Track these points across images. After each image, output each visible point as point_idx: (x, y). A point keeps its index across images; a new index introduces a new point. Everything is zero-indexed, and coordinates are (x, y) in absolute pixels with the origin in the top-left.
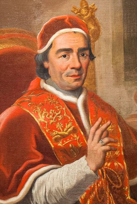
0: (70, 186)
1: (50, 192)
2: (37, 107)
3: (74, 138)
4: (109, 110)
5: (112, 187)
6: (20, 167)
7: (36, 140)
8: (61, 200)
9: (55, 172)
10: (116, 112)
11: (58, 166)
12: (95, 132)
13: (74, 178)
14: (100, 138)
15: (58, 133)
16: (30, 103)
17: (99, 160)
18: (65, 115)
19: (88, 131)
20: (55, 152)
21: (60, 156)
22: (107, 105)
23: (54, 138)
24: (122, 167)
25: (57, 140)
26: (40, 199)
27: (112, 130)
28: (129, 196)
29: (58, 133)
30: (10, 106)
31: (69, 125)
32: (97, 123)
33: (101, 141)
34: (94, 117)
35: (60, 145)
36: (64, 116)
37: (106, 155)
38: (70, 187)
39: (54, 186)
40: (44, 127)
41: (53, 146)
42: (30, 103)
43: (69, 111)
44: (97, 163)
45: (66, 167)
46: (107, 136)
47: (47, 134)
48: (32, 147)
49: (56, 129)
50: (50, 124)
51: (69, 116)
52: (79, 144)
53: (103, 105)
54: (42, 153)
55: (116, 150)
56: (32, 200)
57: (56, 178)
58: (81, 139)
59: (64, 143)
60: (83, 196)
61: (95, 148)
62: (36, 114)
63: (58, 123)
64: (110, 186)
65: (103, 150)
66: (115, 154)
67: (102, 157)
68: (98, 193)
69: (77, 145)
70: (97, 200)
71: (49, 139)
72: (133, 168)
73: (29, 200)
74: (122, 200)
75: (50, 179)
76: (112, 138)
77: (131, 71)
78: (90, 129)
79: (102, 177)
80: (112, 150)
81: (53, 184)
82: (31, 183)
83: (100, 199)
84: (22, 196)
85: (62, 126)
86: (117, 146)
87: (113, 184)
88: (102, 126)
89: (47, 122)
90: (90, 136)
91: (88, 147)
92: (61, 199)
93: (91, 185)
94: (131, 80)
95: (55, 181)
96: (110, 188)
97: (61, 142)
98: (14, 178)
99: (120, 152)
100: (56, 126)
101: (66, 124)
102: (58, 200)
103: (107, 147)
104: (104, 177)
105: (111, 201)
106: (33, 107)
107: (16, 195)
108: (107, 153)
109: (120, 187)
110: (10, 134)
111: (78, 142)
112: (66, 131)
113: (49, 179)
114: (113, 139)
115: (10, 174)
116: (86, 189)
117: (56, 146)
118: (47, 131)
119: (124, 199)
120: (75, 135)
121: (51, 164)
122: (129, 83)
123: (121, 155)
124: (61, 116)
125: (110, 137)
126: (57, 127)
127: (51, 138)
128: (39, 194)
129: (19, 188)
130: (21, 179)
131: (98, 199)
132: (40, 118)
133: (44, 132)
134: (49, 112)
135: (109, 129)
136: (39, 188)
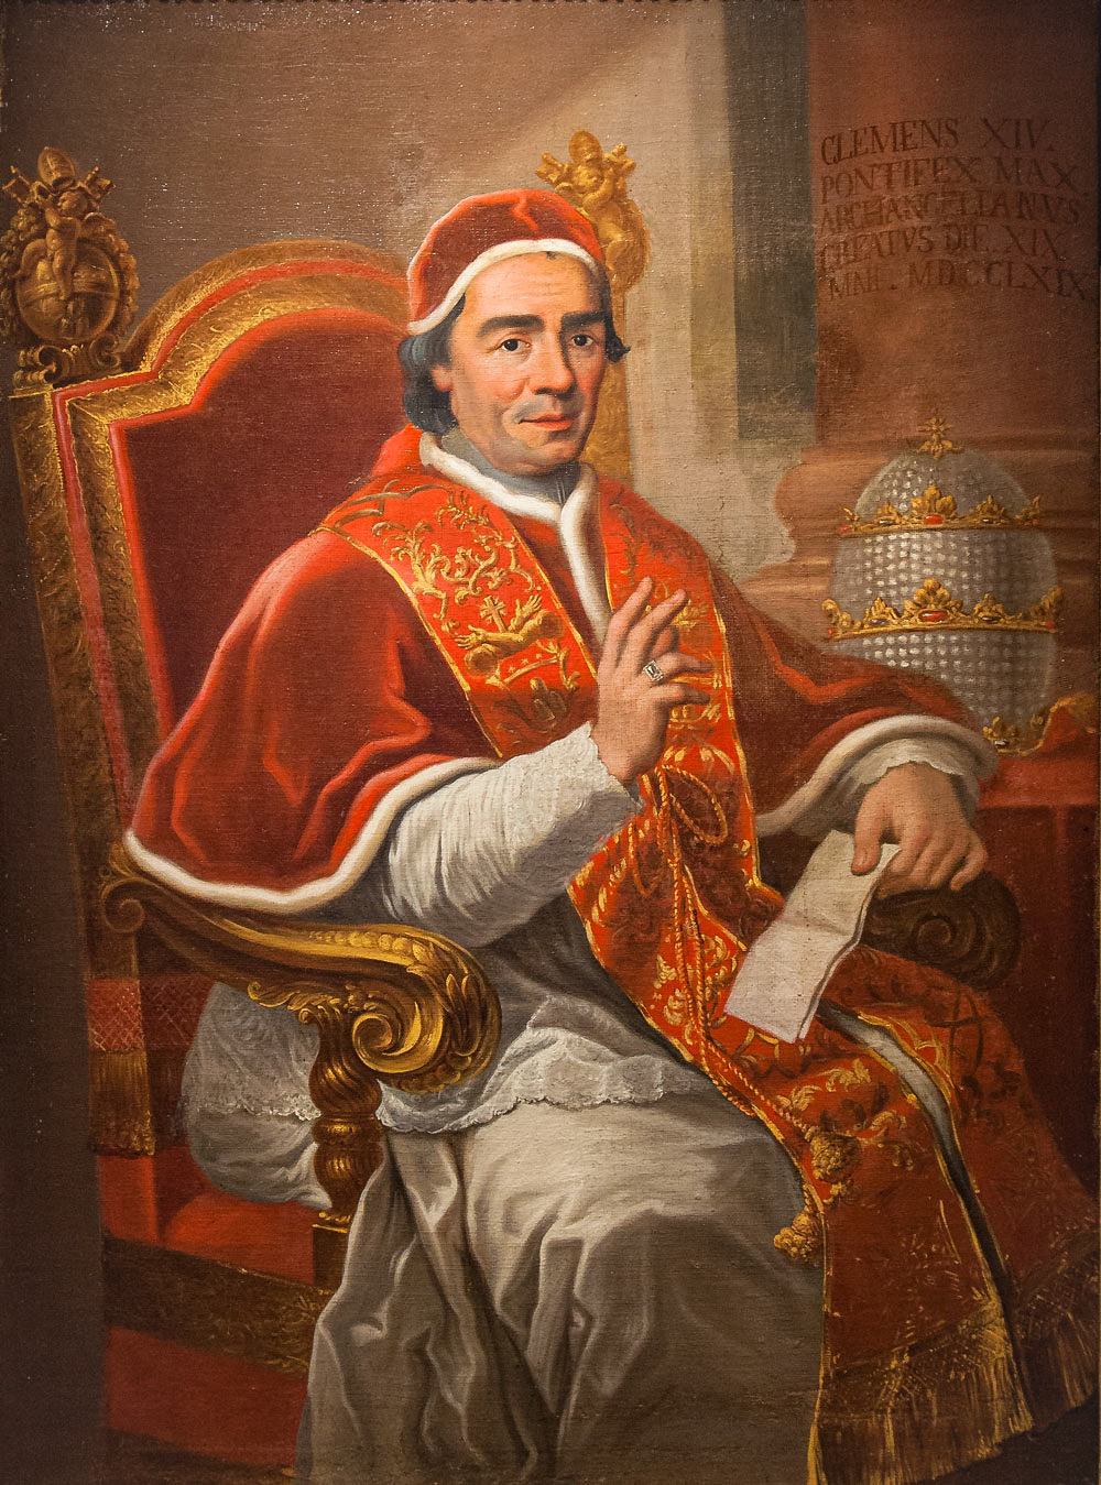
0: (531, 837)
1: (457, 860)
2: (408, 539)
3: (547, 655)
4: (681, 550)
5: (693, 843)
6: (341, 767)
7: (402, 663)
8: (497, 889)
9: (476, 783)
10: (704, 556)
11: (486, 762)
12: (627, 633)
13: (546, 807)
14: (646, 657)
15: (485, 637)
16: (381, 524)
17: (643, 739)
18: (512, 567)
19: (599, 630)
20: (476, 709)
21: (493, 726)
22: (672, 530)
23: (472, 655)
24: (730, 766)
25: (482, 663)
26: (418, 889)
27: (693, 624)
28: (755, 876)
29: (485, 637)
30: (303, 535)
31: (528, 608)
32: (635, 600)
33: (650, 669)
34: (623, 576)
35: (493, 680)
36: (509, 573)
37: (667, 722)
38: (533, 843)
39: (470, 836)
40: (435, 616)
41: (466, 688)
42: (381, 524)
43: (528, 551)
44: (634, 752)
45: (518, 764)
46: (673, 647)
47: (446, 639)
48: (387, 691)
49: (480, 623)
50: (457, 601)
51: (528, 571)
52: (567, 677)
53: (655, 532)
54: (425, 712)
55: (707, 702)
56: (389, 892)
57: (479, 806)
58: (573, 661)
59: (508, 675)
60: (581, 876)
61: (627, 695)
62: (404, 566)
63: (485, 599)
64: (685, 836)
65: (710, 413)
66: (703, 715)
67: (652, 725)
68: (640, 865)
69: (560, 682)
70: (633, 890)
71: (452, 660)
72: (770, 770)
73: (376, 891)
74: (729, 890)
75: (455, 811)
76: (692, 654)
77: (764, 403)
78: (608, 622)
79: (652, 804)
80: (691, 702)
81: (468, 829)
82: (386, 826)
83: (645, 887)
84: (351, 874)
85: (501, 612)
86: (710, 687)
87: (696, 829)
88: (653, 608)
89: (443, 596)
90: (609, 650)
91: (601, 689)
92: (500, 887)
93: (612, 835)
94: (763, 435)
95: (473, 817)
96: (684, 846)
97: (498, 672)
98: (318, 806)
99: (723, 710)
100: (477, 612)
101: (518, 602)
102: (487, 891)
103: (672, 692)
104: (660, 803)
105: (688, 896)
106: (393, 539)
107: (329, 873)
108: (674, 714)
109: (721, 840)
110: (306, 640)
111: (561, 672)
112: (518, 629)
113: (451, 810)
114: (697, 658)
115: (303, 793)
116: (594, 849)
117: (479, 687)
118: (445, 628)
119: (736, 887)
120: (551, 646)
121: (460, 755)
122: (755, 446)
123: (724, 721)
124: (497, 573)
125: (685, 652)
126: (482, 614)
127: (458, 655)
128: (413, 870)
129: (338, 846)
130: (347, 811)
131: (639, 886)
132: (417, 580)
133: (433, 634)
134: (452, 557)
135: (681, 621)
136: (416, 845)
